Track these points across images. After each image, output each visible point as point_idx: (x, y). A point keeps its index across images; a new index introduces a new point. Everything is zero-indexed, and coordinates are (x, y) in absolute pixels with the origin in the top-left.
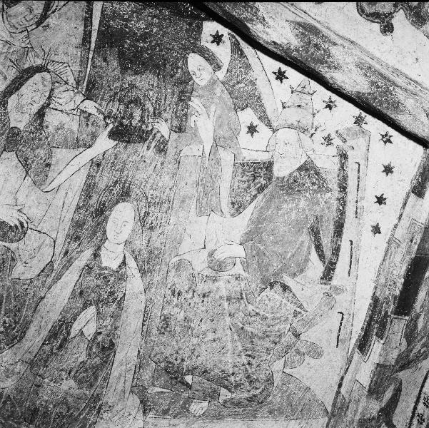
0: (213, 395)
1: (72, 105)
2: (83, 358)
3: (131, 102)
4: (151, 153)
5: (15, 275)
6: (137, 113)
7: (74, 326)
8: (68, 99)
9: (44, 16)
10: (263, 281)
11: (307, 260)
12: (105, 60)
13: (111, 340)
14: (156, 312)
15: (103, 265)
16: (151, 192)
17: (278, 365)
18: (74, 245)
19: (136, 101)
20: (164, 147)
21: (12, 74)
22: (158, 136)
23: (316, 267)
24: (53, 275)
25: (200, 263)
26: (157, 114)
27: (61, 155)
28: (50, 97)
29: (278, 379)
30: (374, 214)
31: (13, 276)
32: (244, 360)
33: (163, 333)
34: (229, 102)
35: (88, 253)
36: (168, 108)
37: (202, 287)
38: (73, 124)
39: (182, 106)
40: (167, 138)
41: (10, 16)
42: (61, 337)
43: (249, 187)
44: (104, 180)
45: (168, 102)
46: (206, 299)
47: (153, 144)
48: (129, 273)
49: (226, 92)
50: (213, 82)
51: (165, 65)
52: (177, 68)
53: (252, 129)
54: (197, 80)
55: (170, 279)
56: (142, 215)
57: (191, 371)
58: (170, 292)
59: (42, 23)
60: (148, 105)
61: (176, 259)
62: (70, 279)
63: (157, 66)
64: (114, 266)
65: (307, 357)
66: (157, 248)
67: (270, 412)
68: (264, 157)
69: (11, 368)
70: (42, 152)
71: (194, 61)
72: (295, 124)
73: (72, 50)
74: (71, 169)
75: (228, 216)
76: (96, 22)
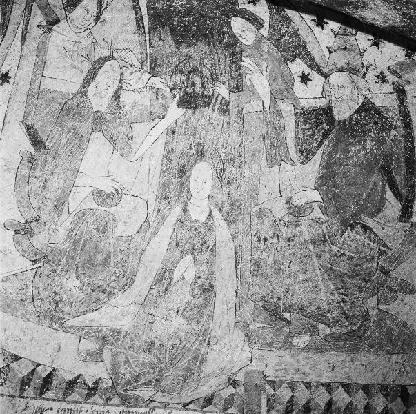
0: (314, 330)
1: (141, 84)
2: (188, 298)
3: (190, 72)
4: (216, 114)
5: (118, 233)
6: (198, 81)
7: (176, 272)
8: (137, 78)
9: (99, 13)
11: (383, 199)
12: (160, 39)
13: (210, 283)
14: (247, 257)
15: (193, 219)
16: (224, 151)
17: (372, 302)
18: (164, 204)
19: (195, 70)
20: (227, 107)
21: (86, 67)
22: (220, 98)
24: (150, 230)
25: (279, 210)
26: (215, 79)
27: (140, 129)
28: (121, 81)
29: (373, 314)
31: (116, 235)
33: (256, 276)
34: (279, 56)
35: (177, 211)
36: (223, 72)
37: (285, 232)
38: (145, 100)
39: (235, 67)
40: (228, 100)
41: (73, 20)
42: (166, 282)
43: (313, 134)
44: (180, 145)
45: (222, 67)
46: (291, 243)
47: (217, 107)
48: (216, 223)
49: (273, 47)
50: (259, 40)
51: (212, 34)
52: (224, 34)
53: (305, 79)
54: (243, 41)
55: (255, 227)
56: (219, 171)
57: (289, 308)
58: (255, 239)
59: (99, 19)
60: (206, 72)
61: (257, 208)
62: (166, 231)
63: (206, 36)
64: (203, 218)
65: (400, 295)
66: (236, 201)
68: (322, 103)
69: (126, 309)
70: (123, 129)
71: (237, 24)
72: (345, 66)
73: (131, 37)
74: (151, 139)
75: (299, 164)
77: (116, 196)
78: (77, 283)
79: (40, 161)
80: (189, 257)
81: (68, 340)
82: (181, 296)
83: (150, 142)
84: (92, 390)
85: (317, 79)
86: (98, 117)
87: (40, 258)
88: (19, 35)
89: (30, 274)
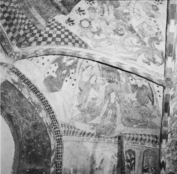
0: (137, 124)
6: (111, 79)
8: (99, 78)
9: (92, 68)
10: (142, 104)
11: (148, 101)
14: (122, 109)
17: (148, 119)
21: (90, 76)
23: (150, 103)
25: (129, 101)
27: (100, 86)
29: (149, 121)
30: (158, 94)
32: (141, 118)
35: (108, 101)
37: (130, 105)
38: (101, 81)
44: (108, 89)
53: (132, 80)
57: (132, 119)
62: (106, 105)
64: (114, 102)
65: (154, 118)
67: (149, 127)
70: (97, 86)
74: (103, 88)
76: (101, 67)
77: (96, 99)
78: (89, 115)
79: (82, 94)
80: (111, 110)
81: (88, 126)
82: (109, 117)
83: (102, 89)
84: (93, 135)
85: (134, 80)
86: (92, 85)
87: (82, 111)
88: (78, 73)
89: (81, 114)
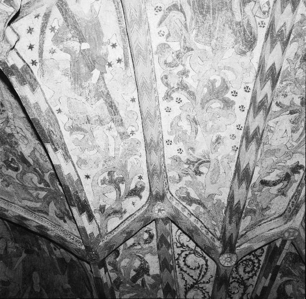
1: (13, 245)
18: (25, 285)
27: (14, 259)
35: (30, 287)
64: (39, 291)
74: (18, 263)
